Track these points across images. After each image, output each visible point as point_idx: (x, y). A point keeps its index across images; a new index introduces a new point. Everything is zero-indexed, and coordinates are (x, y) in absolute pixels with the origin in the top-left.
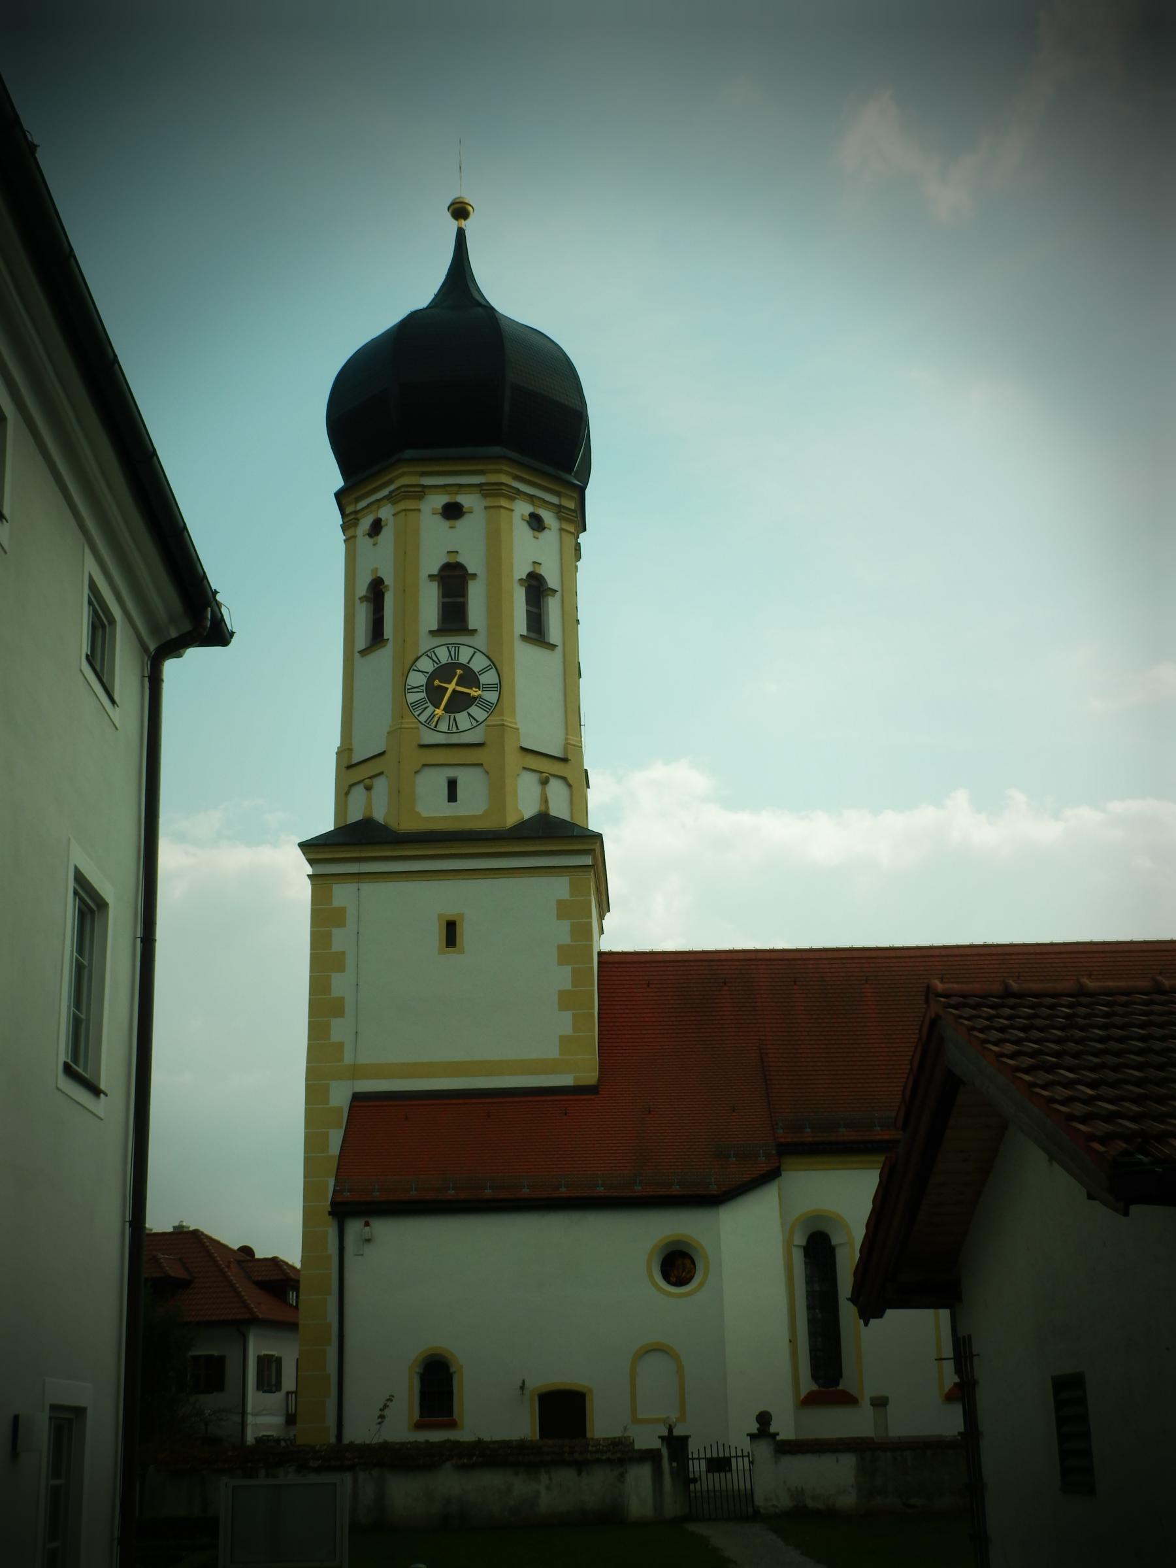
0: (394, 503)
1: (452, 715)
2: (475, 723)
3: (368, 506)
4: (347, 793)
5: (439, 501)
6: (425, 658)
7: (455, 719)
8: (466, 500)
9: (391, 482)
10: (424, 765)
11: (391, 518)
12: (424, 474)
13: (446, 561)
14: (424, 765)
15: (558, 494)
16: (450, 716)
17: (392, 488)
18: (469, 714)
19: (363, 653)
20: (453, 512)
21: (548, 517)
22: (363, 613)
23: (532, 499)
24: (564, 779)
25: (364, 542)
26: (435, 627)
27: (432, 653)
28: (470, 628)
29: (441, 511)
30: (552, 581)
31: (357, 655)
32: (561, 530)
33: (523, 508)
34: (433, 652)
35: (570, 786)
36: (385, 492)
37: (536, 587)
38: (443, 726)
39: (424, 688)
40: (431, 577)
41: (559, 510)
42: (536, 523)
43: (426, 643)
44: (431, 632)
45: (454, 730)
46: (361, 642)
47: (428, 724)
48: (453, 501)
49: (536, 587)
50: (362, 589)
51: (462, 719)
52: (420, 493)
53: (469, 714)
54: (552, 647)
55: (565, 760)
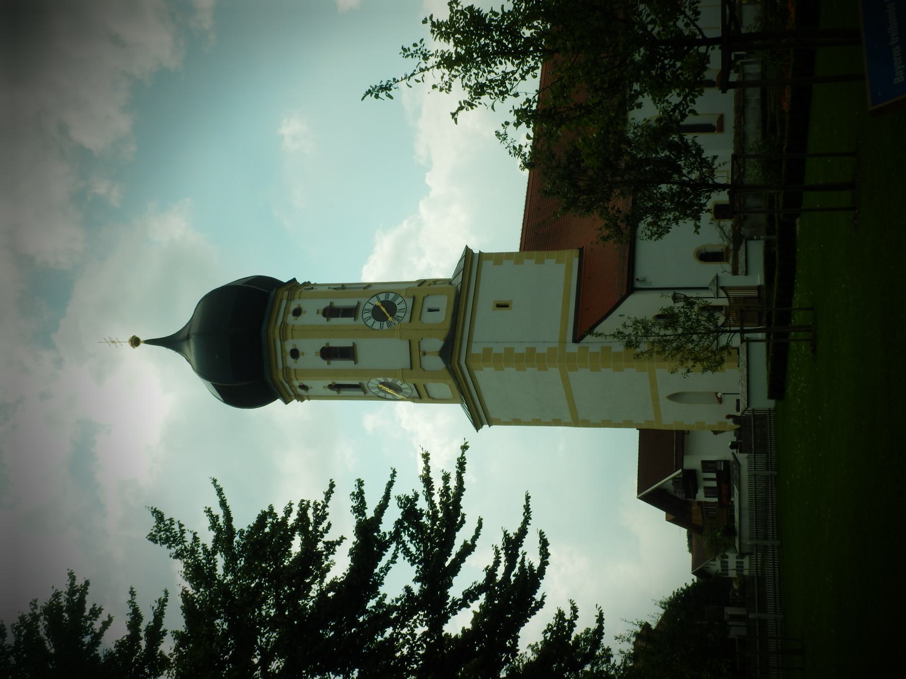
0: (292, 381)
3: (293, 391)
4: (433, 399)
5: (290, 361)
8: (289, 347)
9: (281, 382)
10: (421, 367)
11: (299, 381)
12: (277, 367)
13: (319, 357)
15: (281, 301)
17: (285, 383)
19: (365, 392)
20: (295, 354)
21: (293, 306)
22: (344, 393)
23: (285, 315)
24: (424, 298)
25: (310, 392)
26: (353, 362)
28: (352, 345)
29: (295, 360)
30: (325, 304)
31: (366, 395)
32: (299, 298)
33: (290, 318)
35: (428, 295)
36: (287, 385)
37: (330, 312)
40: (328, 364)
41: (290, 299)
42: (297, 312)
44: (355, 364)
46: (362, 393)
48: (289, 354)
49: (330, 312)
50: (334, 393)
52: (286, 370)
54: (359, 303)
55: (414, 298)
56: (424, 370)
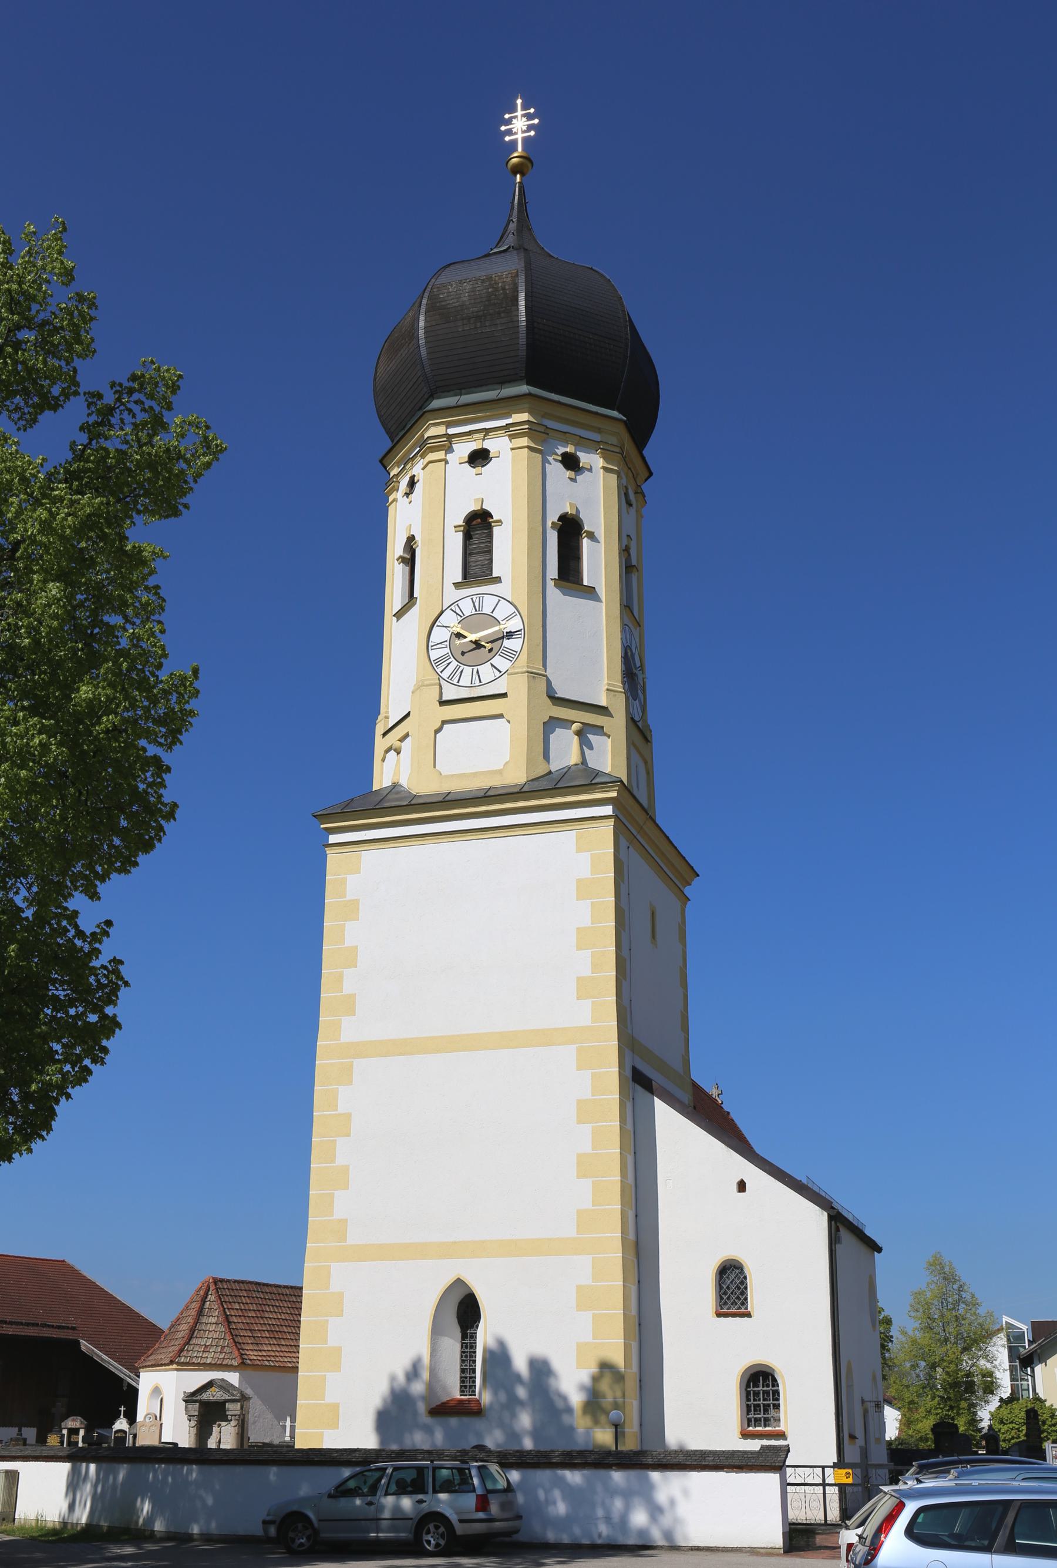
1: (475, 668)
2: (498, 674)
6: (448, 612)
7: (478, 672)
8: (497, 445)
10: (444, 722)
14: (444, 722)
16: (473, 669)
18: (492, 665)
27: (456, 606)
34: (457, 605)
38: (465, 680)
39: (448, 643)
43: (452, 594)
44: (457, 585)
45: (477, 683)
47: (451, 680)
51: (486, 672)
53: (492, 665)
56: (437, 731)
